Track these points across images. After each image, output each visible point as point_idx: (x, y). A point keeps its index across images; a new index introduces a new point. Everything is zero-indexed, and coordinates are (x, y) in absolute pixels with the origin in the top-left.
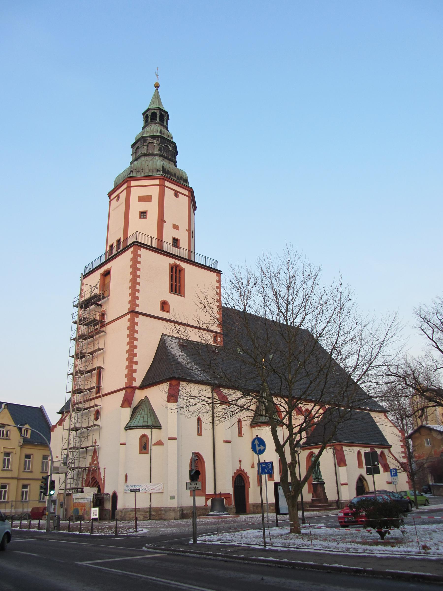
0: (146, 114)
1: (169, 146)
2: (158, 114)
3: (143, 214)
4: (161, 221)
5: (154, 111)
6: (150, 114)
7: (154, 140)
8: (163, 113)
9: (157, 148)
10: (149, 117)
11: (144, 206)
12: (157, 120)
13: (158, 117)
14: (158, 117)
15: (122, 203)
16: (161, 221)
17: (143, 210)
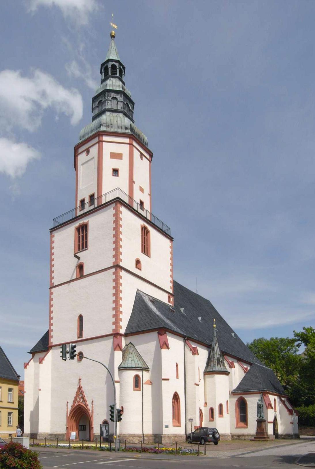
0: (105, 65)
1: (129, 104)
2: (118, 67)
3: (116, 172)
4: (131, 182)
5: (114, 63)
6: (110, 66)
7: (117, 95)
8: (121, 67)
9: (120, 105)
10: (110, 69)
11: (116, 164)
12: (117, 73)
13: (118, 70)
14: (118, 70)
15: (93, 158)
16: (131, 182)
17: (116, 167)
